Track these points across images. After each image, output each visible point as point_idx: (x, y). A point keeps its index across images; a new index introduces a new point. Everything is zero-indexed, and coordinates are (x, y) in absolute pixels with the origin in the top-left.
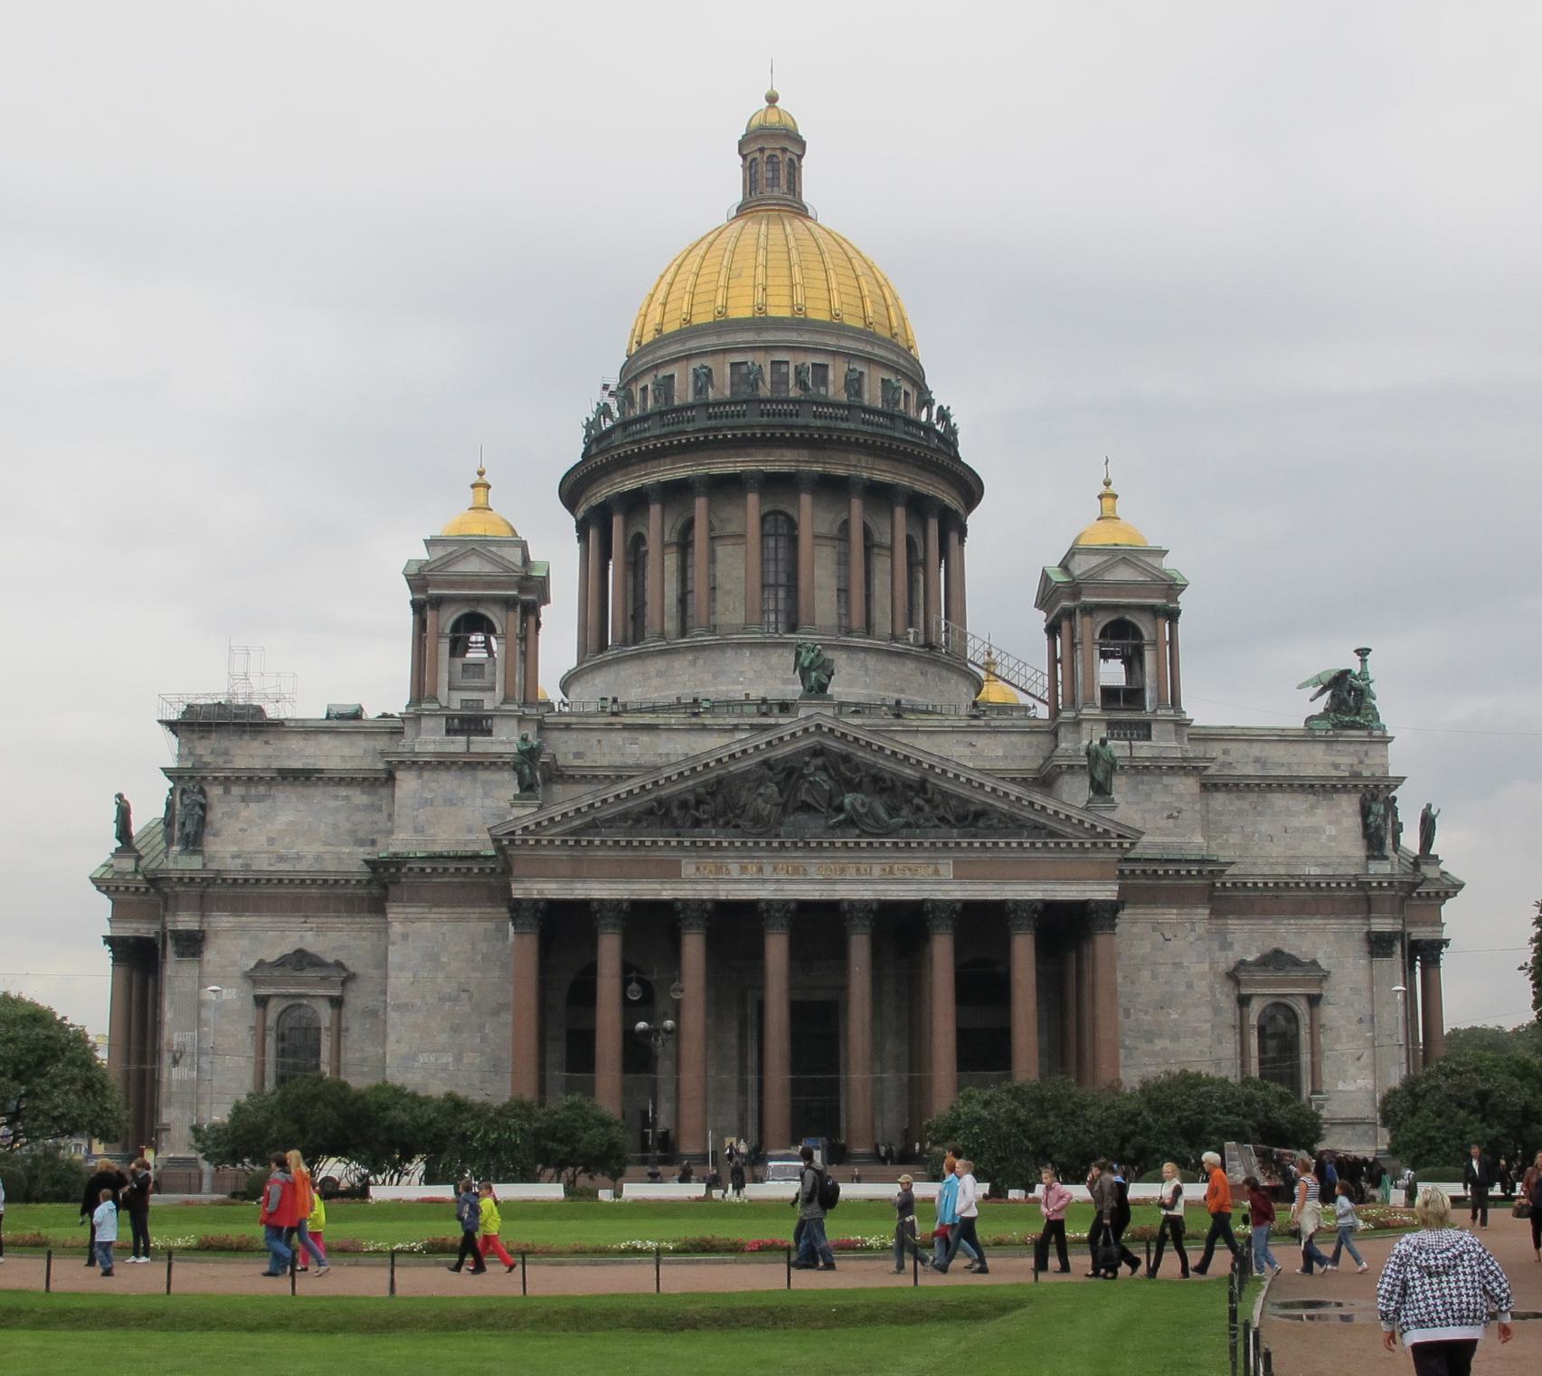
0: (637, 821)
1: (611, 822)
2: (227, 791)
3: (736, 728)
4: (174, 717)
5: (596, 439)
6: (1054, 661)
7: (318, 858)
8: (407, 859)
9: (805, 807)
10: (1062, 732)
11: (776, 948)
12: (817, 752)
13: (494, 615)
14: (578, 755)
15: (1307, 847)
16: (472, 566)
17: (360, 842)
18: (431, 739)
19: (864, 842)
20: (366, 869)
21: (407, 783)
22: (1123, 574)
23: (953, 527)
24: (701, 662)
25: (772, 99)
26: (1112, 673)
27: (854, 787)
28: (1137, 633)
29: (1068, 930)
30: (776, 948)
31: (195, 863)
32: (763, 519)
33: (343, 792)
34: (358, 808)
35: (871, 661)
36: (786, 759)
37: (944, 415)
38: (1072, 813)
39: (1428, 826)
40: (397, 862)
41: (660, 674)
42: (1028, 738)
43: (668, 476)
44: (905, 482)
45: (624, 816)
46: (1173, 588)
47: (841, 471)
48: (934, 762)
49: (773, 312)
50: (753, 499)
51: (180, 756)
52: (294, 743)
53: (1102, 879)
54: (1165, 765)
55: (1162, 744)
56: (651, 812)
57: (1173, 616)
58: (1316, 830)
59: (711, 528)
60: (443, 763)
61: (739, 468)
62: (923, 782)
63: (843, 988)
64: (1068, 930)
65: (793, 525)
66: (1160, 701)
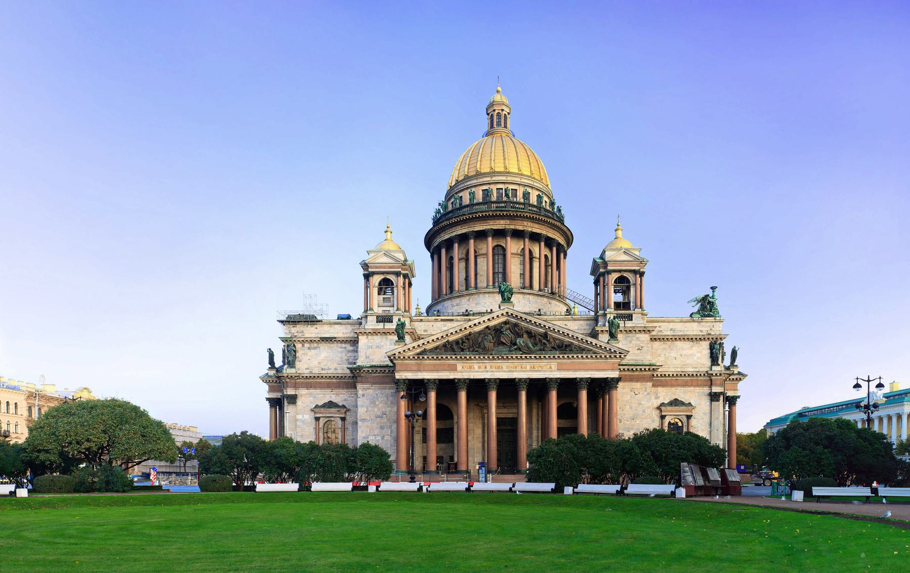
1: (431, 351)
2: (303, 346)
4: (285, 319)
5: (436, 222)
6: (597, 294)
8: (363, 367)
11: (493, 396)
12: (506, 323)
14: (425, 331)
19: (523, 356)
20: (348, 371)
21: (363, 340)
23: (561, 251)
26: (619, 298)
27: (520, 336)
28: (628, 281)
29: (600, 389)
30: (493, 396)
32: (493, 249)
33: (344, 345)
34: (349, 351)
35: (531, 297)
36: (495, 326)
37: (559, 211)
38: (602, 344)
40: (360, 368)
42: (586, 322)
43: (459, 232)
44: (544, 232)
45: (436, 348)
48: (550, 325)
52: (326, 328)
53: (613, 370)
54: (637, 329)
56: (445, 345)
59: (475, 252)
60: (375, 333)
62: (545, 335)
63: (518, 413)
64: (600, 389)
65: (504, 250)
66: (636, 307)
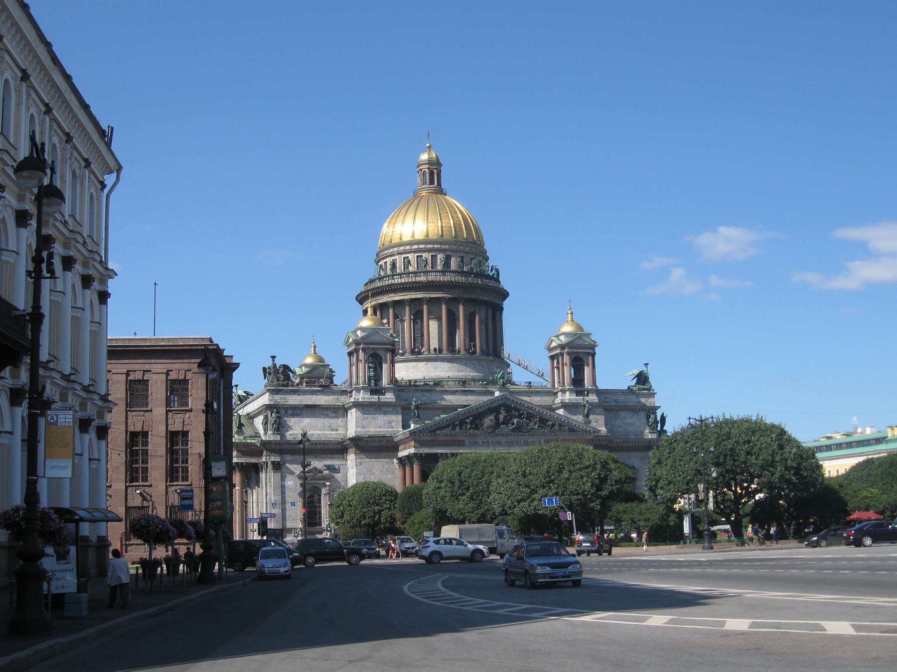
0: (454, 429)
2: (286, 412)
6: (553, 369)
7: (319, 435)
9: (503, 423)
10: (560, 394)
12: (503, 405)
13: (381, 353)
15: (630, 429)
16: (376, 338)
17: (333, 430)
22: (580, 342)
24: (429, 363)
31: (278, 438)
36: (495, 407)
39: (663, 419)
41: (413, 367)
43: (413, 297)
44: (491, 299)
46: (593, 346)
47: (473, 297)
50: (444, 307)
51: (270, 400)
55: (593, 398)
57: (593, 355)
58: (633, 424)
61: (440, 295)
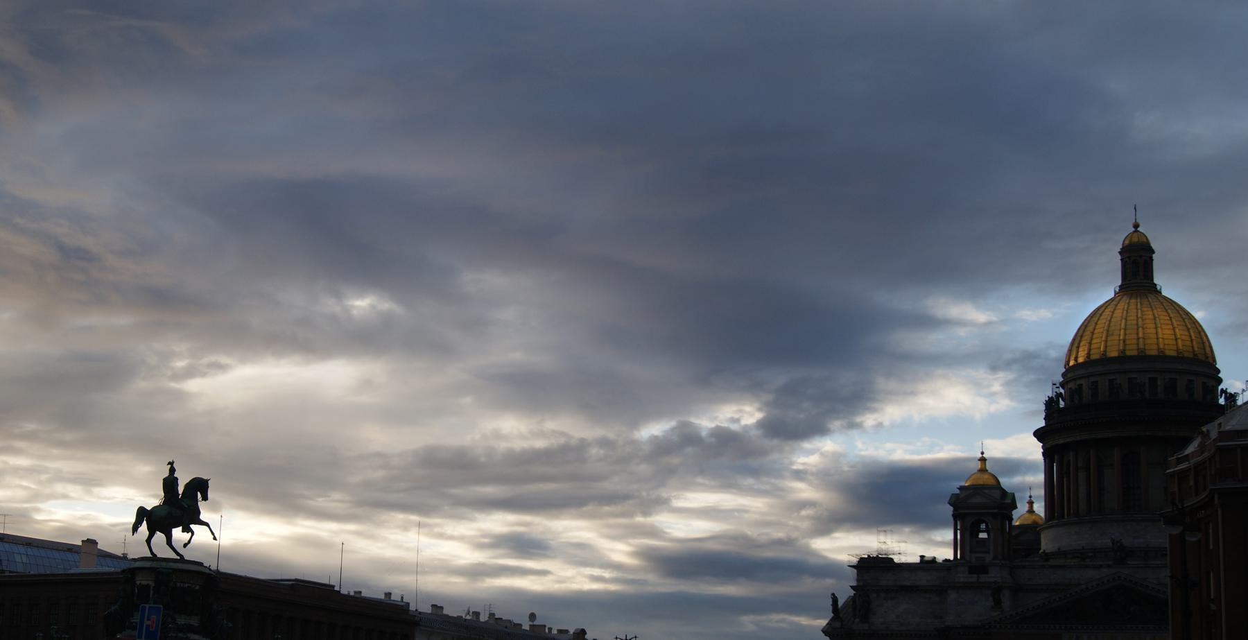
3: (1101, 566)
16: (978, 500)
18: (962, 576)
21: (952, 596)
25: (1136, 226)
49: (1128, 353)
